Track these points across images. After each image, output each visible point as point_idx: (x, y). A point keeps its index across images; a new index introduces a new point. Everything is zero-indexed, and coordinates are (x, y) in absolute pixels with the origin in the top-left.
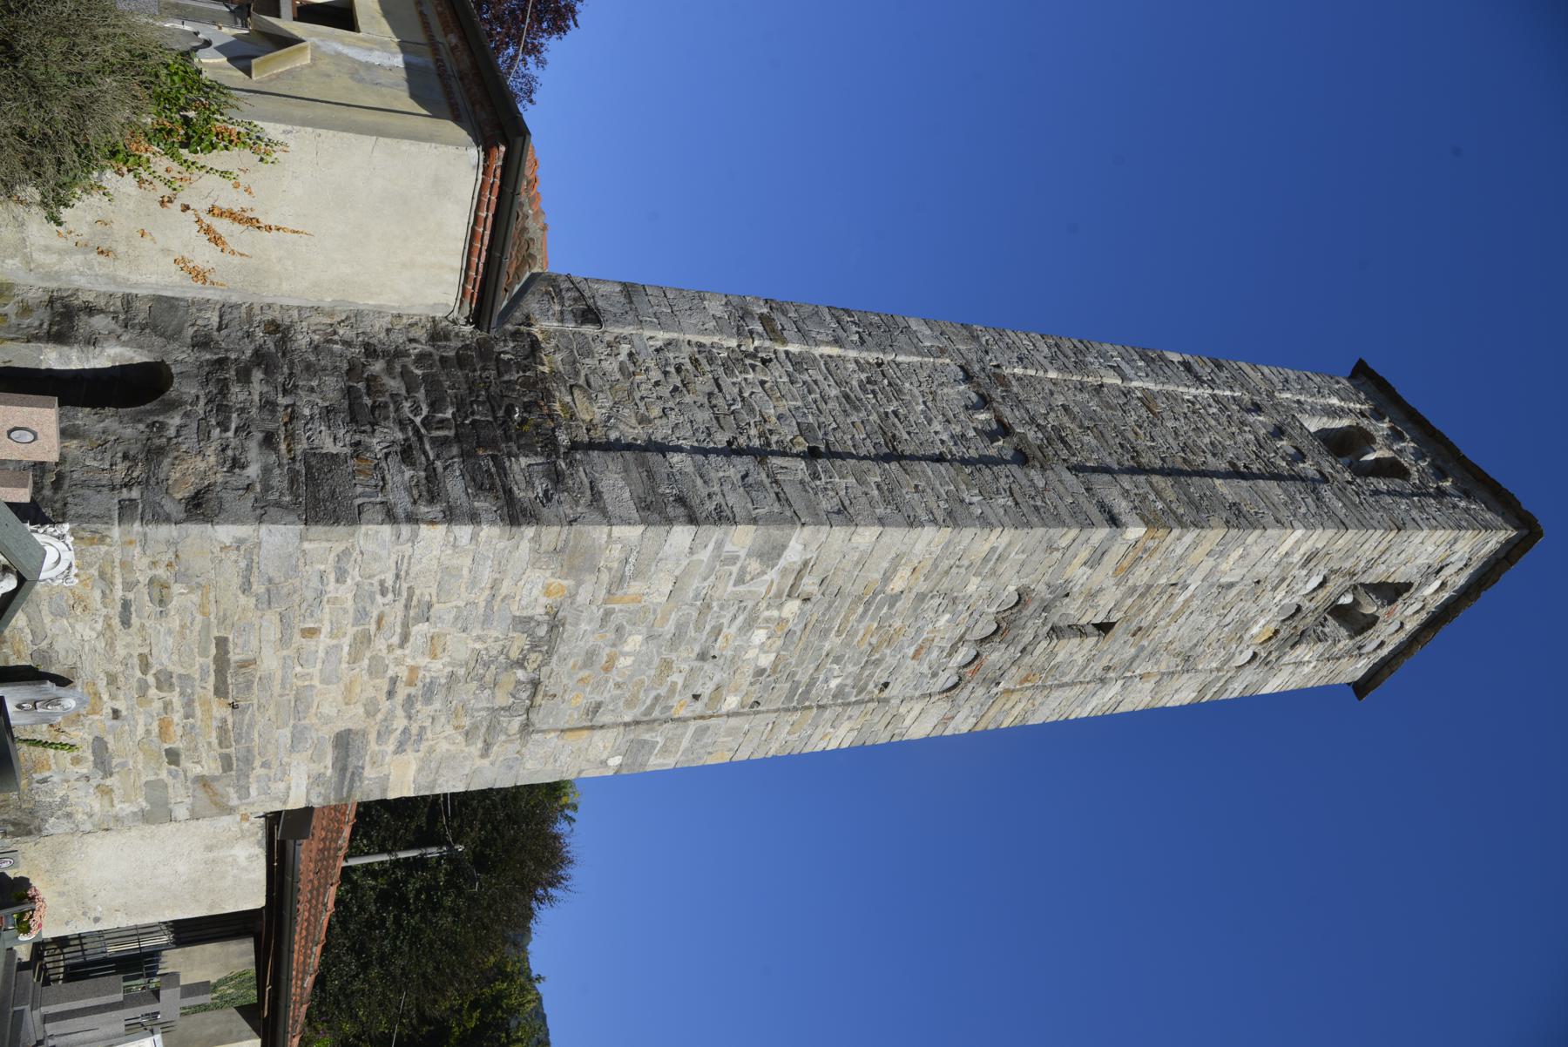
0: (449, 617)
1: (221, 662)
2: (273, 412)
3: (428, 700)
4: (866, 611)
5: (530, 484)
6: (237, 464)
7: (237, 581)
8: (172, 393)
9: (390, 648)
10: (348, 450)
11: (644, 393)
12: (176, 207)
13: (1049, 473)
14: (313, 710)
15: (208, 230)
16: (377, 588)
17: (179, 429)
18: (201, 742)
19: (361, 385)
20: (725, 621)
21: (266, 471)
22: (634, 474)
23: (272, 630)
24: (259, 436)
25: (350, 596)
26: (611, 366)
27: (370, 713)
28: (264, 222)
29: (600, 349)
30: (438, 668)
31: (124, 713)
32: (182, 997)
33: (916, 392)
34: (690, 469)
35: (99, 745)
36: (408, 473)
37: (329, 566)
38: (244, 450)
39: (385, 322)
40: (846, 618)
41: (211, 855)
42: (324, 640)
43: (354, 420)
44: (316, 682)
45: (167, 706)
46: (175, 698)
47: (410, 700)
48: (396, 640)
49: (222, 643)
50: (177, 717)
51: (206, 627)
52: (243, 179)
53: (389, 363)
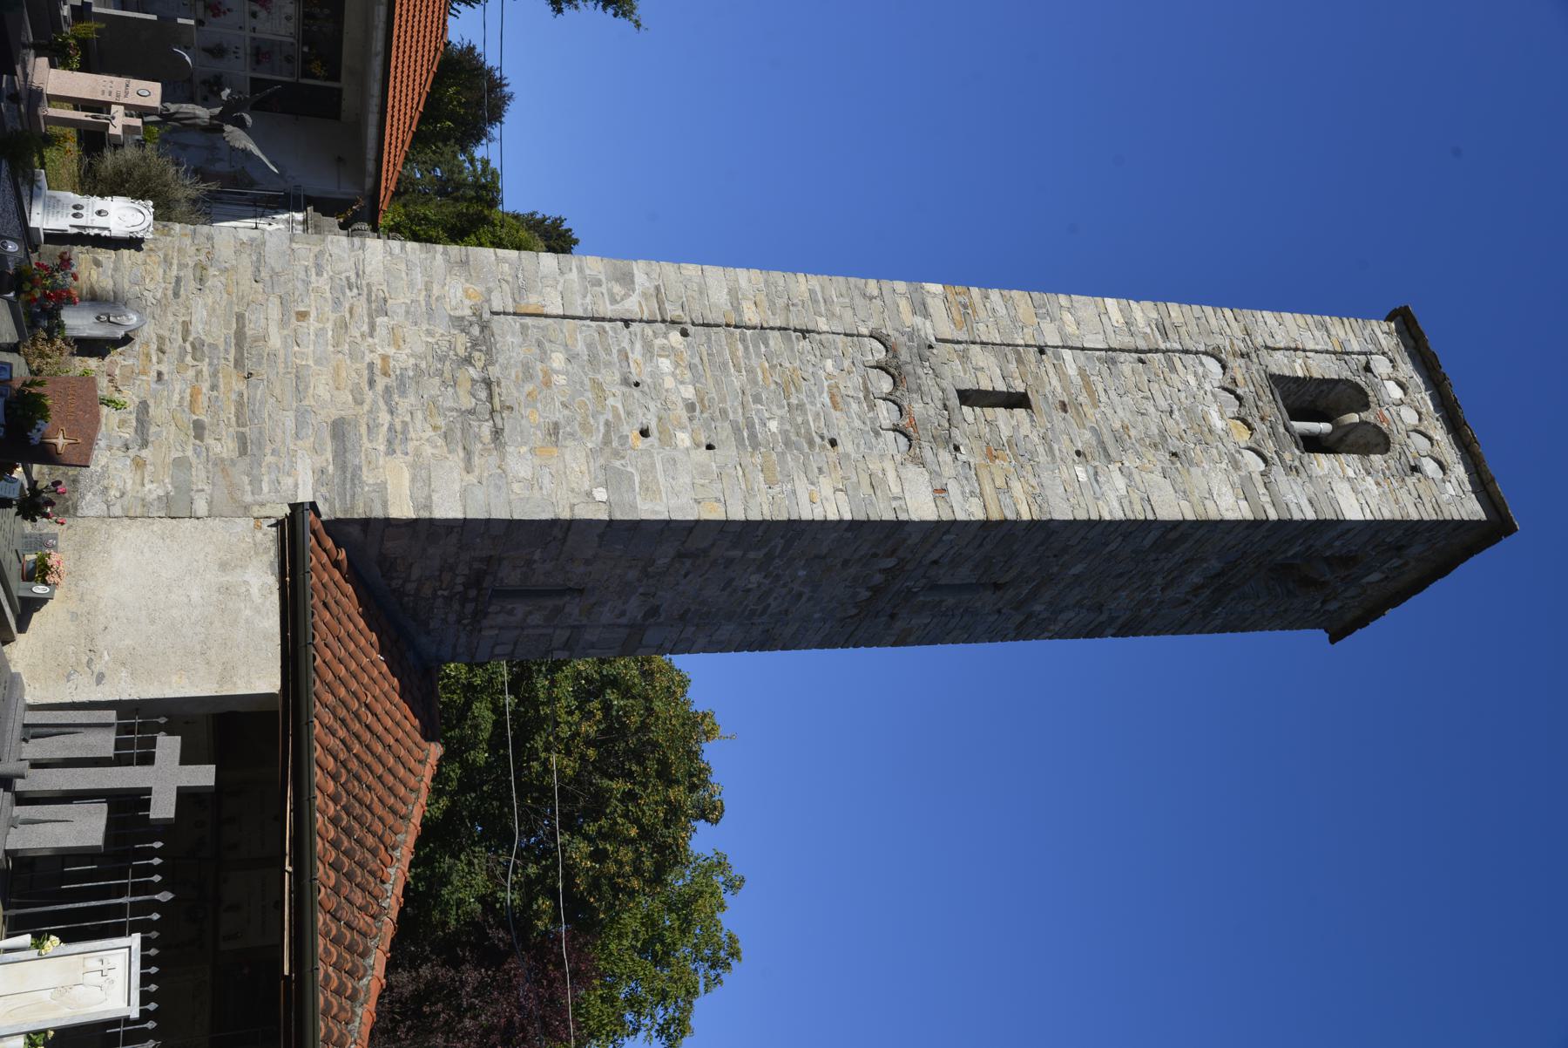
0: (402, 311)
1: (240, 335)
3: (403, 394)
4: (746, 348)
7: (249, 275)
9: (362, 335)
14: (311, 391)
16: (345, 283)
18: (223, 416)
20: (625, 344)
23: (274, 312)
25: (327, 288)
27: (359, 402)
30: (403, 359)
31: (166, 377)
32: (184, 761)
35: (144, 407)
37: (310, 263)
41: (226, 579)
42: (312, 324)
44: (311, 363)
45: (199, 373)
46: (205, 367)
47: (387, 389)
48: (365, 328)
49: (240, 317)
50: (205, 387)
51: (231, 303)
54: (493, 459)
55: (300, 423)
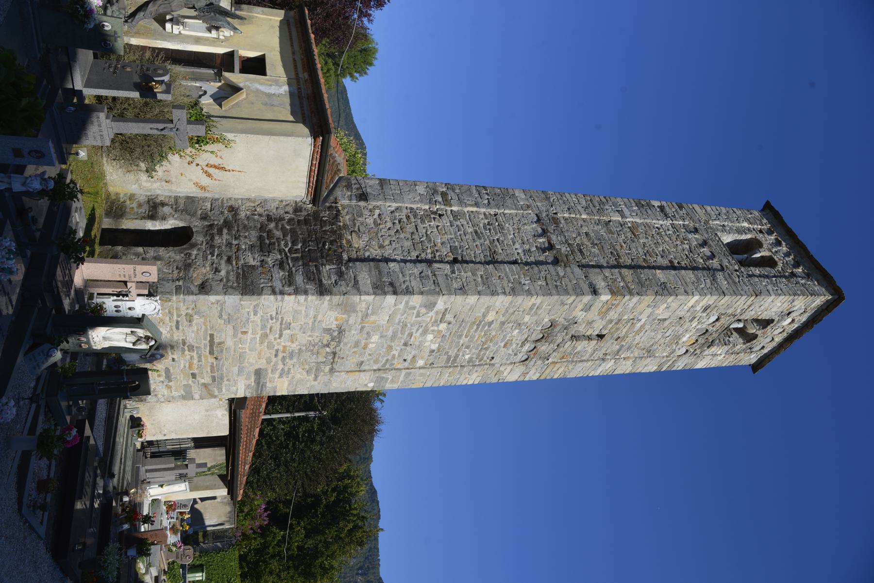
2: (231, 247)
3: (291, 358)
4: (478, 328)
5: (329, 277)
6: (217, 270)
7: (217, 314)
8: (193, 240)
9: (275, 339)
10: (259, 264)
11: (383, 234)
12: (194, 164)
13: (568, 269)
15: (206, 172)
17: (197, 255)
18: (204, 371)
19: (265, 234)
20: (414, 331)
21: (228, 273)
22: (373, 273)
23: (230, 332)
24: (225, 258)
26: (370, 221)
27: (269, 362)
28: (227, 168)
29: (366, 212)
30: (294, 346)
33: (511, 229)
34: (397, 270)
35: (167, 371)
36: (282, 273)
37: (251, 309)
38: (220, 264)
39: (275, 204)
40: (469, 331)
42: (250, 336)
43: (261, 250)
44: (247, 350)
45: (192, 357)
46: (195, 354)
47: (284, 358)
48: (277, 336)
49: (212, 336)
50: (195, 362)
51: (206, 330)
52: (219, 154)
53: (277, 224)
54: (328, 377)
55: (240, 371)
